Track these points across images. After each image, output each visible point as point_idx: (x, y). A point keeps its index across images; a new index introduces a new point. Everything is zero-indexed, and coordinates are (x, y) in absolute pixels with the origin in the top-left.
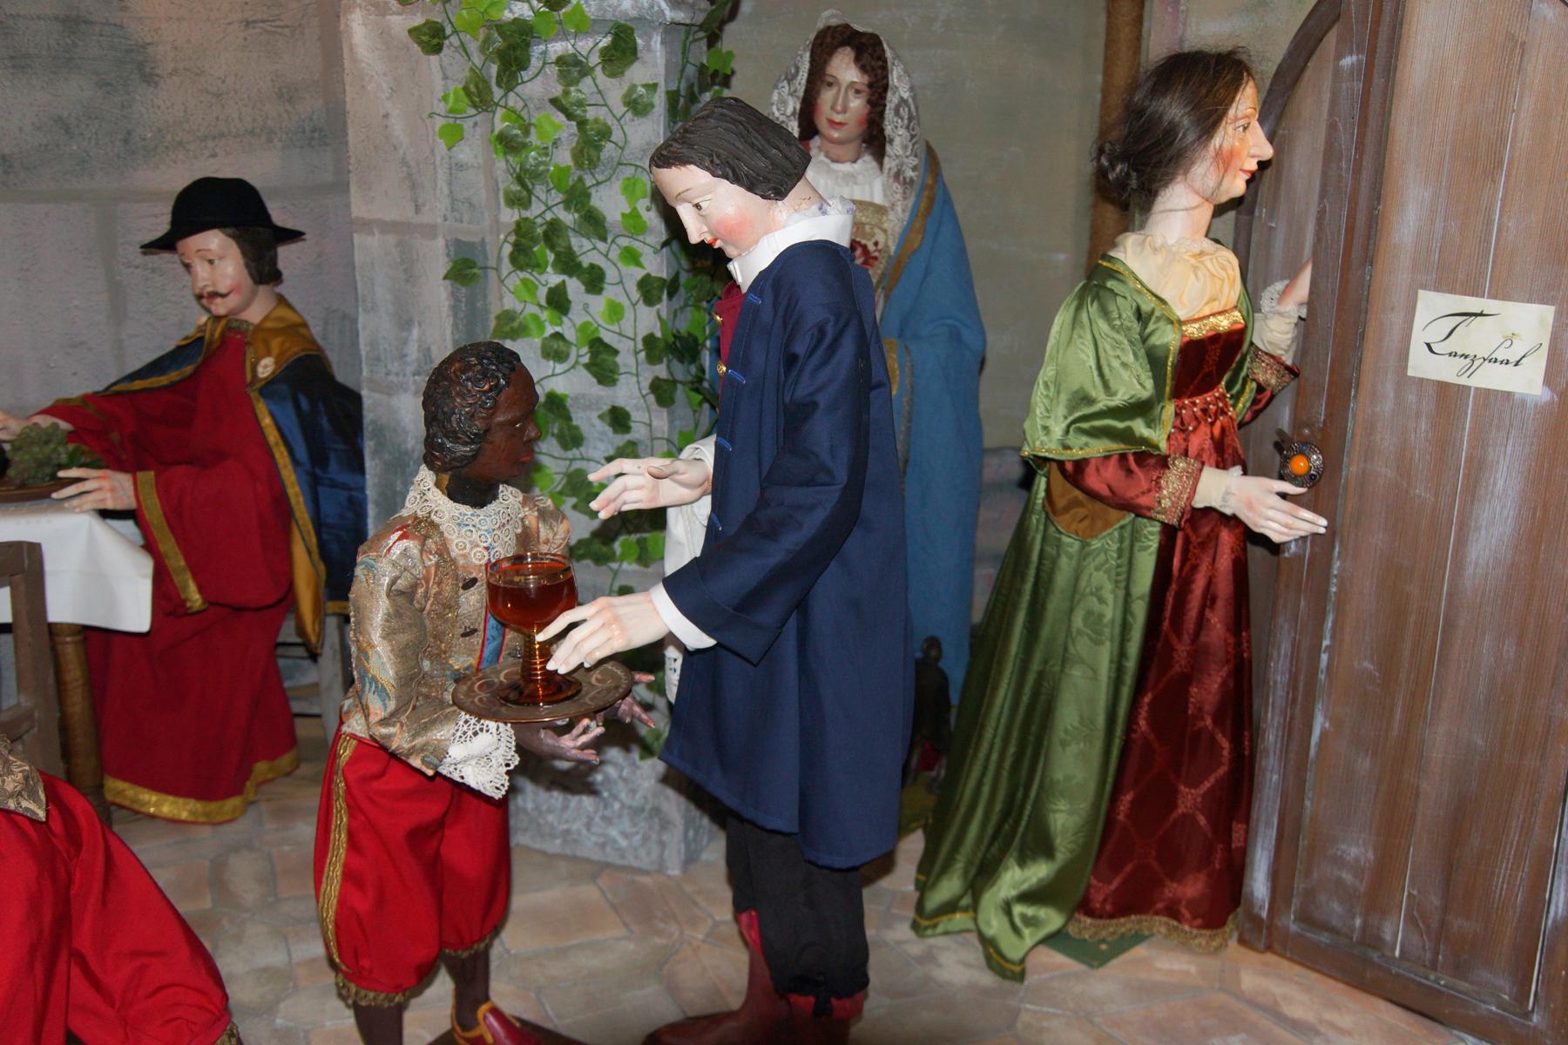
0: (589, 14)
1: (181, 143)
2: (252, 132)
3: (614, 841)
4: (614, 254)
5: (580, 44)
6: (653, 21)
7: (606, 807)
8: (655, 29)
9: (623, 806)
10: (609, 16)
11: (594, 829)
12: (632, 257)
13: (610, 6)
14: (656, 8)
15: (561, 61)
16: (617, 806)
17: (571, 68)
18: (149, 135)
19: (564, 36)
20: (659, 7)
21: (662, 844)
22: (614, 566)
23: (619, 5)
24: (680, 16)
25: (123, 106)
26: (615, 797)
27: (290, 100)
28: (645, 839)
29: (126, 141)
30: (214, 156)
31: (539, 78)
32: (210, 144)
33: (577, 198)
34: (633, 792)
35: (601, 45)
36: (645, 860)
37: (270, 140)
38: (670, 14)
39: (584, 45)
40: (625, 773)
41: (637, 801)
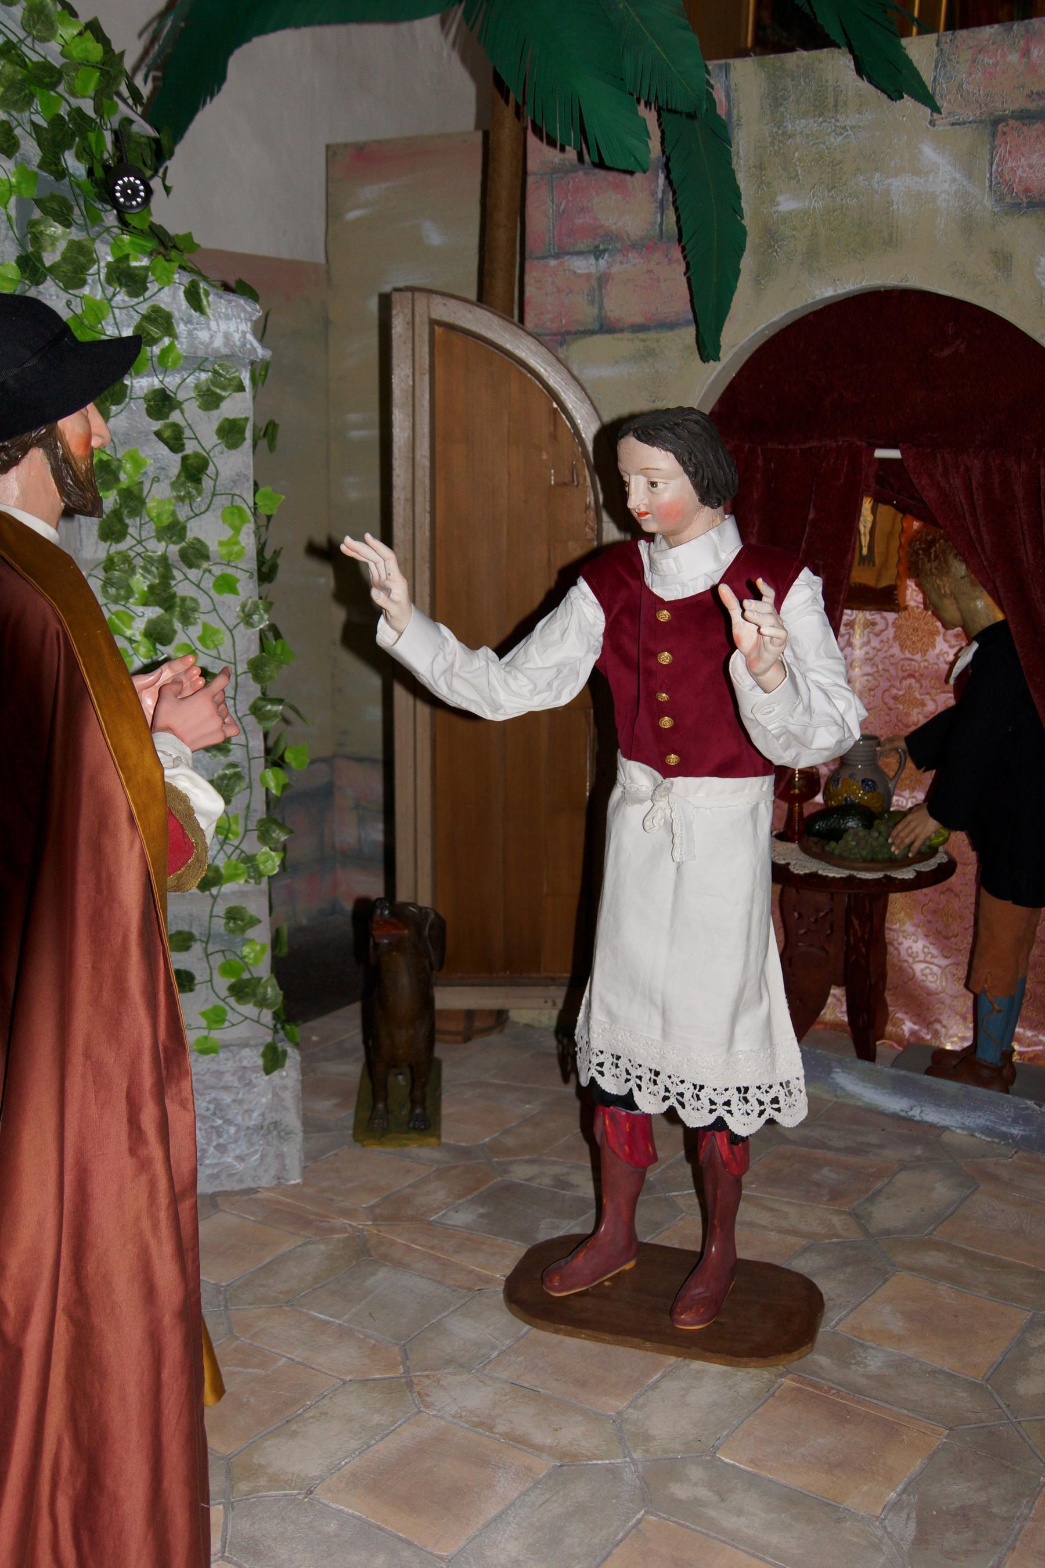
0: (181, 351)
3: (231, 1166)
4: (208, 583)
5: (167, 379)
6: (243, 359)
8: (244, 366)
9: (239, 1128)
10: (201, 353)
12: (227, 584)
13: (202, 343)
14: (248, 346)
15: (146, 399)
19: (154, 372)
20: (252, 345)
21: (280, 1156)
22: (214, 891)
23: (212, 342)
26: (229, 1122)
28: (263, 1157)
31: (123, 413)
33: (174, 530)
34: (249, 1112)
35: (191, 381)
36: (266, 1180)
38: (261, 352)
40: (240, 1096)
41: (255, 1119)
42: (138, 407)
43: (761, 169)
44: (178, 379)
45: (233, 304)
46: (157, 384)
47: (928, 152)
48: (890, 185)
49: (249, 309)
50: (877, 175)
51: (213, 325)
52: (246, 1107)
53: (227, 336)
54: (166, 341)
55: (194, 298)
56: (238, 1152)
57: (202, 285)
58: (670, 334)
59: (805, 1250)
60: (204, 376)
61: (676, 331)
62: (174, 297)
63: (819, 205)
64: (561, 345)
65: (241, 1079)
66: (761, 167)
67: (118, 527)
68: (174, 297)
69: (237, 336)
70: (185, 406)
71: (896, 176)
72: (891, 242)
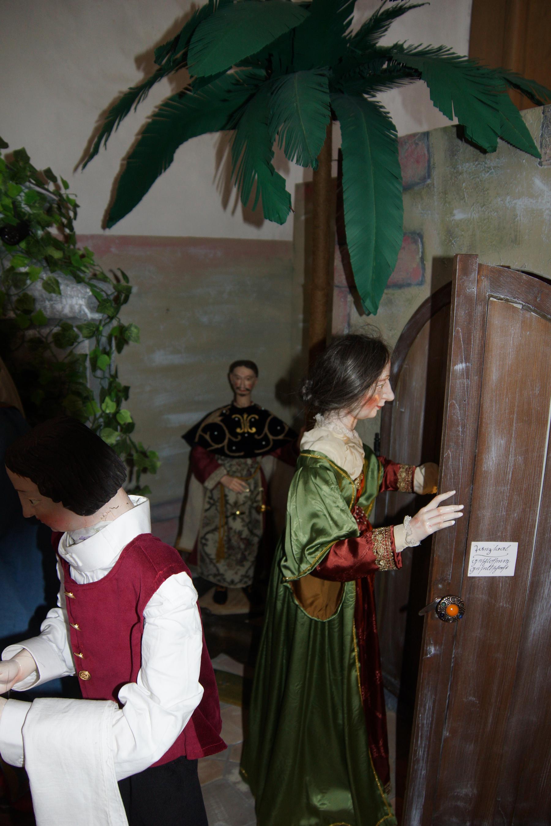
14: (82, 312)
20: (84, 311)
24: (97, 316)
38: (90, 315)
43: (446, 194)
45: (75, 289)
46: (38, 335)
47: (538, 183)
48: (516, 204)
49: (83, 292)
50: (508, 198)
51: (64, 301)
63: (476, 216)
66: (445, 193)
69: (77, 307)
71: (519, 198)
72: (516, 241)
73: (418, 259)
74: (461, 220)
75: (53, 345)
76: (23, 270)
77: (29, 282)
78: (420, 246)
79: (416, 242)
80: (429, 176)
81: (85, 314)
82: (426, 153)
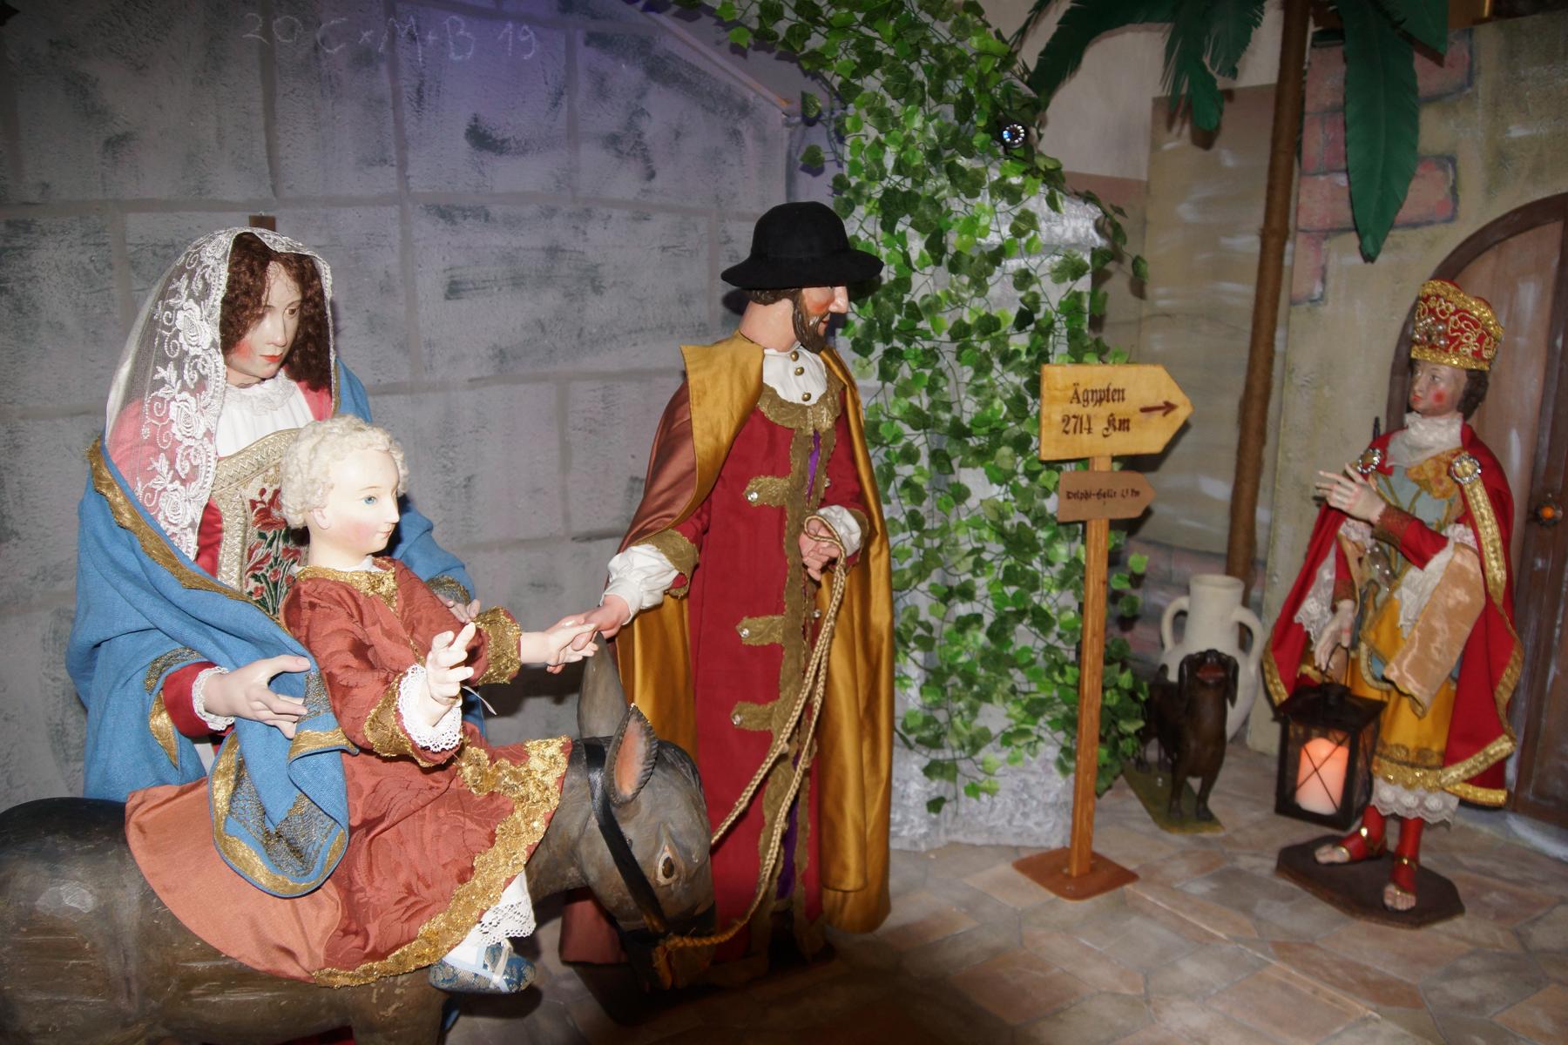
1: (615, 336)
2: (660, 327)
5: (1031, 261)
7: (1025, 805)
8: (1086, 251)
9: (1039, 802)
10: (1055, 242)
11: (1015, 823)
15: (1014, 275)
16: (1034, 803)
17: (1024, 279)
18: (594, 331)
25: (579, 311)
26: (1032, 797)
27: (687, 304)
28: (1055, 826)
29: (579, 336)
30: (635, 345)
32: (634, 336)
34: (1047, 792)
37: (672, 333)
38: (1100, 242)
39: (1034, 262)
41: (1051, 798)
42: (1009, 280)
44: (1038, 261)
46: (1024, 266)
51: (1066, 222)
52: (1046, 788)
53: (1075, 230)
54: (1032, 233)
55: (1052, 203)
56: (1037, 819)
57: (1058, 193)
58: (1412, 232)
59: (1471, 954)
60: (1057, 259)
61: (1419, 230)
62: (1039, 204)
64: (1325, 238)
65: (1044, 768)
67: (986, 364)
68: (1039, 204)
69: (1082, 231)
70: (1042, 279)
73: (1446, 189)
74: (1520, 138)
75: (1047, 283)
76: (1015, 180)
77: (1024, 197)
78: (1451, 172)
79: (1444, 168)
80: (1470, 84)
81: (1094, 240)
82: (1467, 55)
